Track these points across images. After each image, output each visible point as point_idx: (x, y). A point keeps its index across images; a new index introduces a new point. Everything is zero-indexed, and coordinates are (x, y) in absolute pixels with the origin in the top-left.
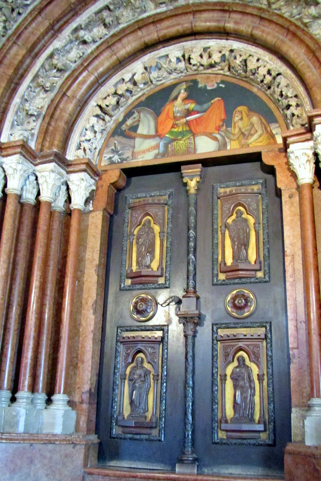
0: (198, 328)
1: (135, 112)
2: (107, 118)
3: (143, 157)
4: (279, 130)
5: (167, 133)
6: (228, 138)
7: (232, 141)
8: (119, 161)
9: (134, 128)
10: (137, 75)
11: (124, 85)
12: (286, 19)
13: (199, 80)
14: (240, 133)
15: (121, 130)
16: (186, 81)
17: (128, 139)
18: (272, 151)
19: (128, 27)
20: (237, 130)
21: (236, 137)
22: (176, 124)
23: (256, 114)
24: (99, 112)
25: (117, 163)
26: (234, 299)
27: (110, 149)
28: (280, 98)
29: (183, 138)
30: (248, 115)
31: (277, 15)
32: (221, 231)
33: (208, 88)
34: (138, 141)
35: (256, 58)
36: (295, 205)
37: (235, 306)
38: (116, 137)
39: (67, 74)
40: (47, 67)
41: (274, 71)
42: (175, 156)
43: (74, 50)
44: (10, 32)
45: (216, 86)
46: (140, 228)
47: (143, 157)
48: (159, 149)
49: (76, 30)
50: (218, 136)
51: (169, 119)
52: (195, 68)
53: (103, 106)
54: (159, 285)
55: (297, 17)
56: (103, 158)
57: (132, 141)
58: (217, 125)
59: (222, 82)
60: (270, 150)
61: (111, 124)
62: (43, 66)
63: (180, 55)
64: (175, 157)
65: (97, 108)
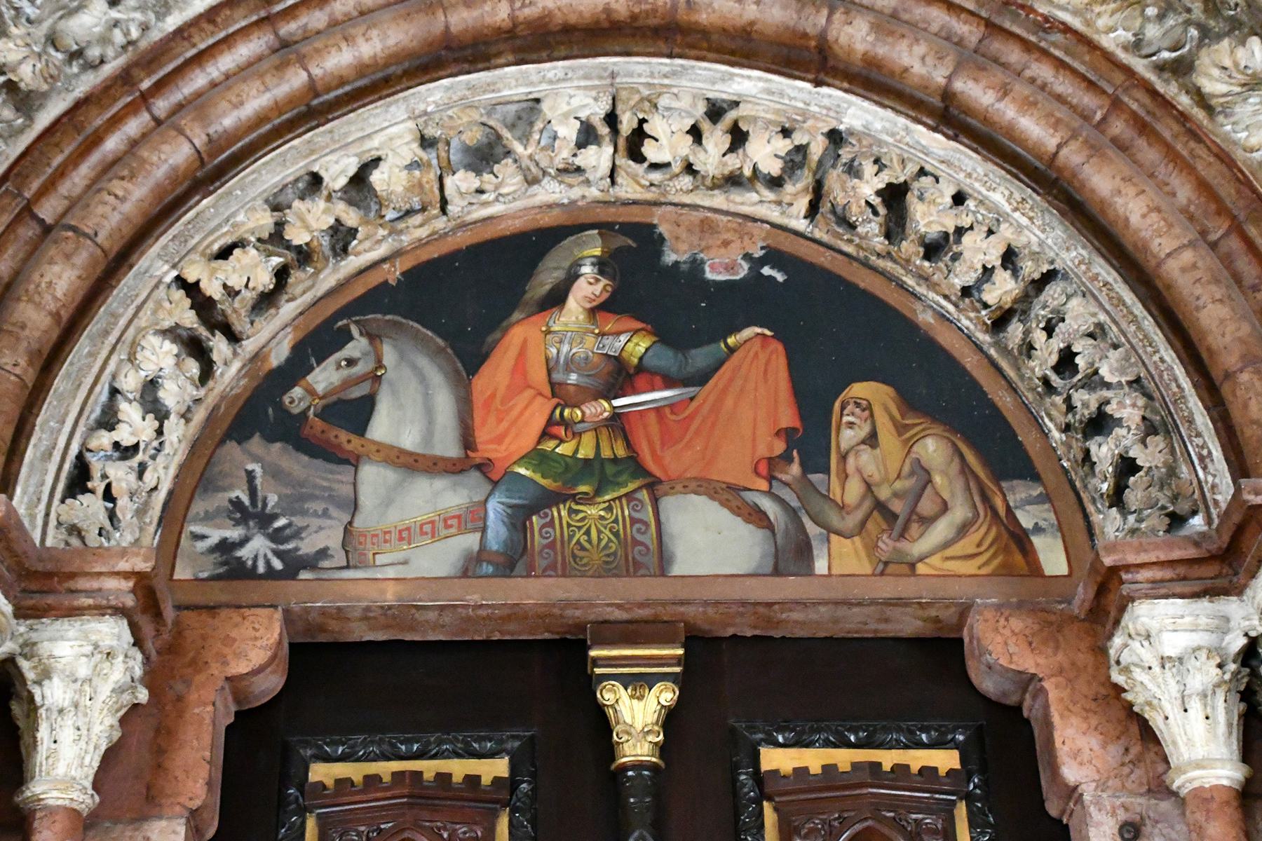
1: (355, 331)
2: (219, 346)
3: (405, 563)
5: (523, 459)
7: (834, 537)
8: (277, 564)
10: (383, 166)
11: (321, 204)
12: (1108, 57)
13: (663, 229)
14: (867, 504)
15: (280, 408)
16: (604, 228)
17: (319, 463)
20: (854, 490)
21: (852, 521)
22: (564, 422)
23: (938, 429)
24: (189, 318)
25: (261, 577)
27: (221, 500)
28: (1055, 380)
29: (598, 492)
30: (901, 429)
31: (1067, 29)
33: (710, 275)
35: (950, 191)
38: (256, 443)
41: (1035, 256)
42: (564, 576)
45: (743, 270)
47: (405, 563)
48: (484, 530)
50: (767, 505)
51: (529, 393)
52: (656, 176)
53: (212, 289)
55: (1166, 55)
56: (184, 541)
57: (345, 473)
58: (762, 451)
59: (773, 256)
60: (1014, 600)
63: (597, 110)
65: (179, 294)
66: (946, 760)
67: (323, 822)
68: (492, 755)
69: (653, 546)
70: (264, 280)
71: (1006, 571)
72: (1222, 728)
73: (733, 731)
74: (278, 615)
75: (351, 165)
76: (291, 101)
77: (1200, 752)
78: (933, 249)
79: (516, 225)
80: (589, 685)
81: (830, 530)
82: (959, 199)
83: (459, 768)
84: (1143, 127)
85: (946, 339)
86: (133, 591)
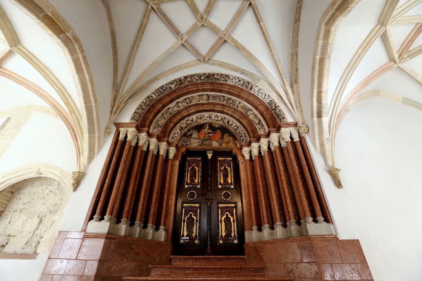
2: (182, 130)
4: (238, 143)
9: (191, 135)
16: (209, 124)
19: (193, 105)
20: (225, 141)
21: (225, 143)
24: (180, 128)
34: (192, 139)
38: (184, 137)
39: (172, 115)
40: (167, 111)
43: (176, 108)
44: (157, 99)
49: (178, 103)
50: (219, 142)
53: (182, 126)
59: (220, 126)
61: (183, 132)
62: (165, 111)
66: (231, 159)
67: (188, 162)
70: (185, 126)
75: (192, 119)
76: (188, 114)
78: (231, 125)
79: (203, 123)
82: (233, 122)
83: (197, 159)
84: (244, 117)
85: (232, 131)
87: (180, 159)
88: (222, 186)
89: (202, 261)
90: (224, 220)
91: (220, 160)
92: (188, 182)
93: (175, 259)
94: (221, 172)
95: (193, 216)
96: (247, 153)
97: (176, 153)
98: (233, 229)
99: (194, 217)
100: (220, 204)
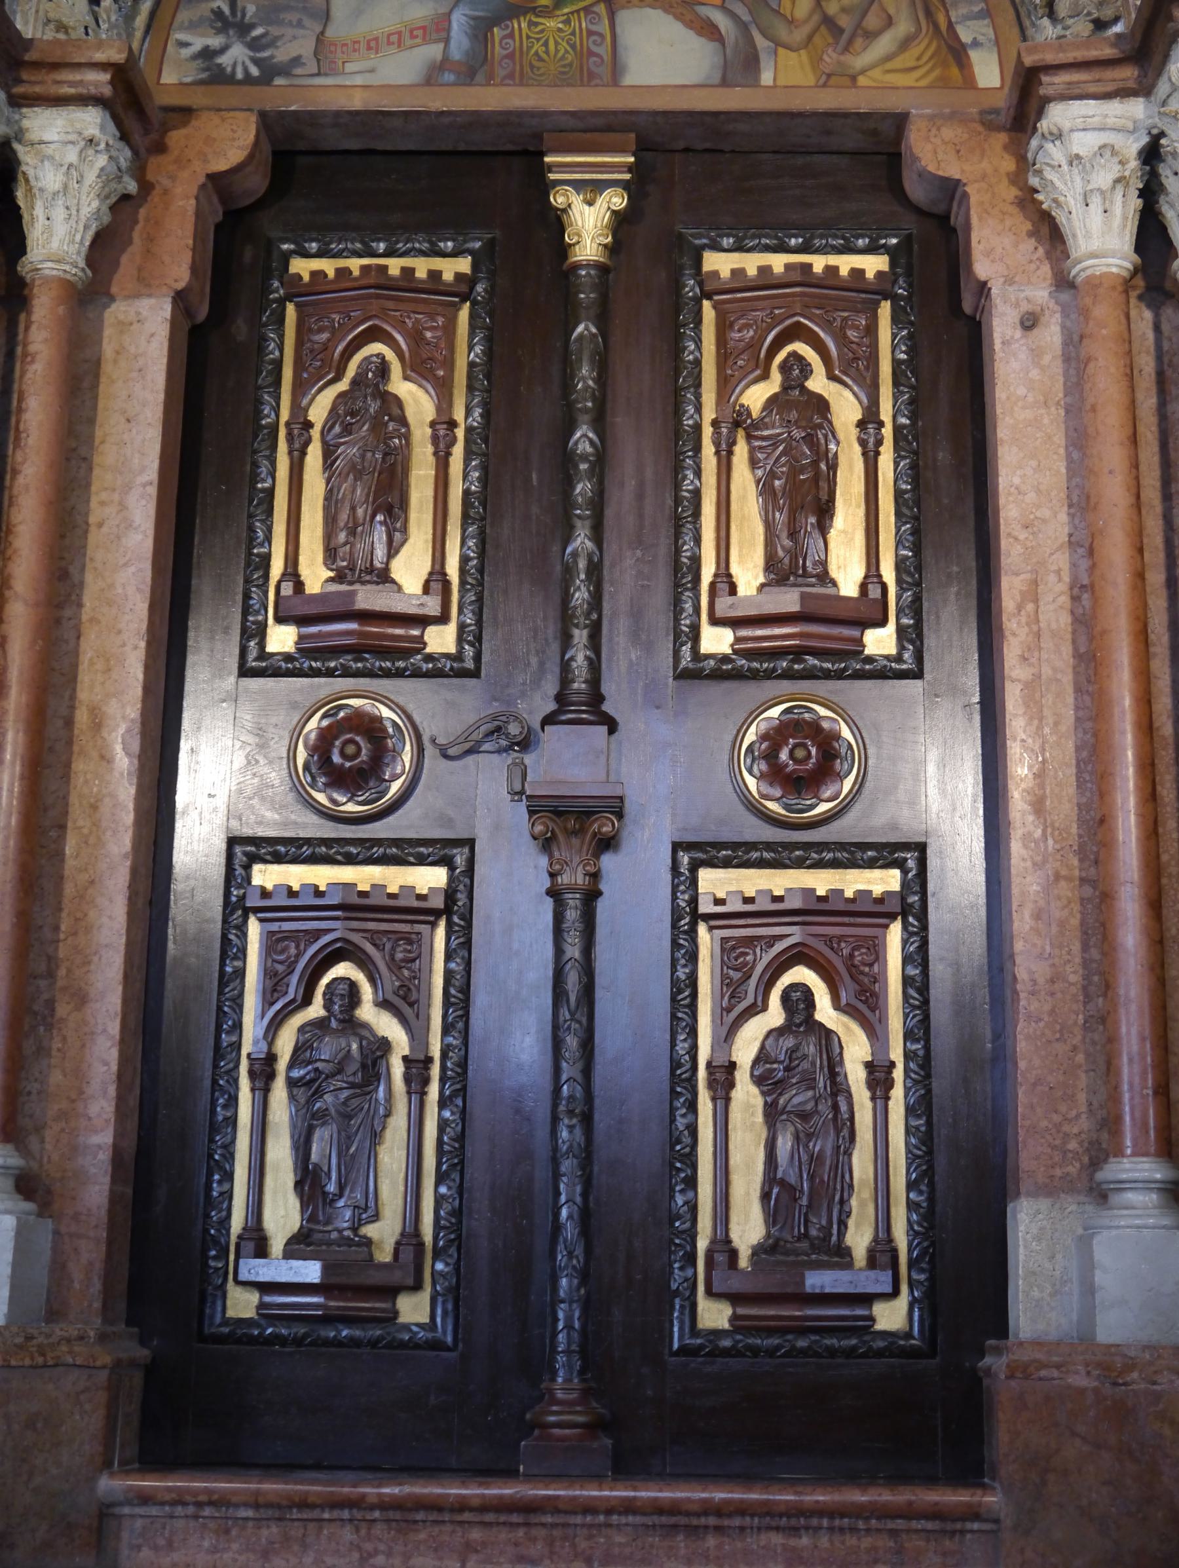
0: (608, 861)
3: (372, 71)
6: (765, 35)
7: (781, 50)
8: (255, 71)
14: (816, 18)
18: (955, 117)
21: (799, 35)
25: (240, 83)
26: (775, 737)
27: (204, 9)
32: (717, 444)
36: (1047, 359)
37: (775, 774)
42: (521, 84)
46: (341, 395)
47: (372, 71)
48: (447, 41)
54: (430, 658)
56: (170, 48)
60: (947, 111)
64: (523, 90)
66: (873, 265)
67: (298, 306)
68: (454, 254)
69: (607, 57)
71: (943, 83)
72: (1117, 221)
73: (680, 235)
74: (253, 118)
77: (1095, 245)
80: (545, 188)
81: (778, 43)
83: (422, 267)
86: (112, 82)
87: (180, 273)
88: (744, 633)
89: (476, 1534)
90: (756, 1062)
91: (725, 274)
92: (299, 586)
93: (154, 1511)
94: (741, 450)
95: (367, 1012)
96: (1103, 178)
97: (132, 187)
98: (862, 1163)
99: (388, 1027)
100: (712, 864)
